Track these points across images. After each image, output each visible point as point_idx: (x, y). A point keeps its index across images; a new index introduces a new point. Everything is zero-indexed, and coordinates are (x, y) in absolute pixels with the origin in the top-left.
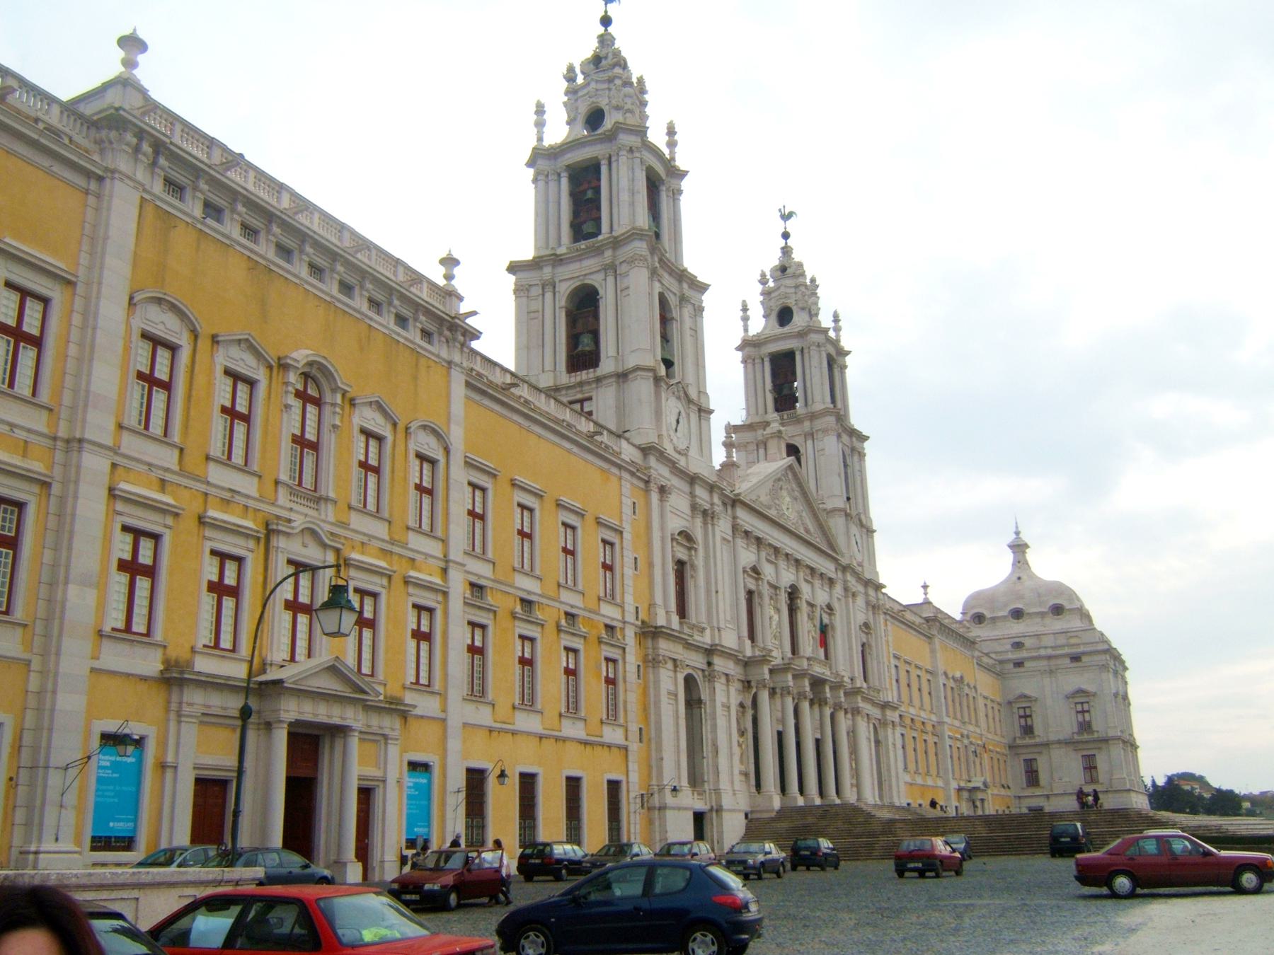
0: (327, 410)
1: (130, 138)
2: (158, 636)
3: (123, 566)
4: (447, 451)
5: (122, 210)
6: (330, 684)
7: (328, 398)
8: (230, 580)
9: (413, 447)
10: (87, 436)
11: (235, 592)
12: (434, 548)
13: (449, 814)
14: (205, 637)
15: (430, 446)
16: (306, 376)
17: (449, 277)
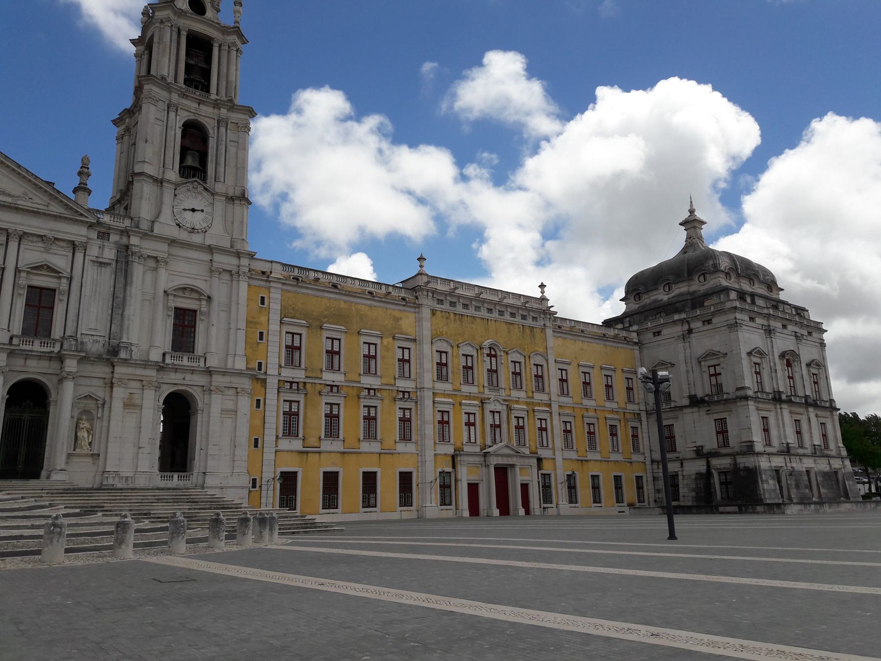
0: (499, 358)
1: (425, 293)
2: (452, 442)
3: (439, 422)
4: (547, 361)
5: (426, 313)
6: (507, 451)
7: (498, 354)
8: (472, 421)
9: (532, 362)
10: (425, 386)
11: (474, 424)
12: (544, 397)
13: (560, 491)
14: (465, 439)
15: (539, 360)
16: (490, 348)
17: (543, 292)
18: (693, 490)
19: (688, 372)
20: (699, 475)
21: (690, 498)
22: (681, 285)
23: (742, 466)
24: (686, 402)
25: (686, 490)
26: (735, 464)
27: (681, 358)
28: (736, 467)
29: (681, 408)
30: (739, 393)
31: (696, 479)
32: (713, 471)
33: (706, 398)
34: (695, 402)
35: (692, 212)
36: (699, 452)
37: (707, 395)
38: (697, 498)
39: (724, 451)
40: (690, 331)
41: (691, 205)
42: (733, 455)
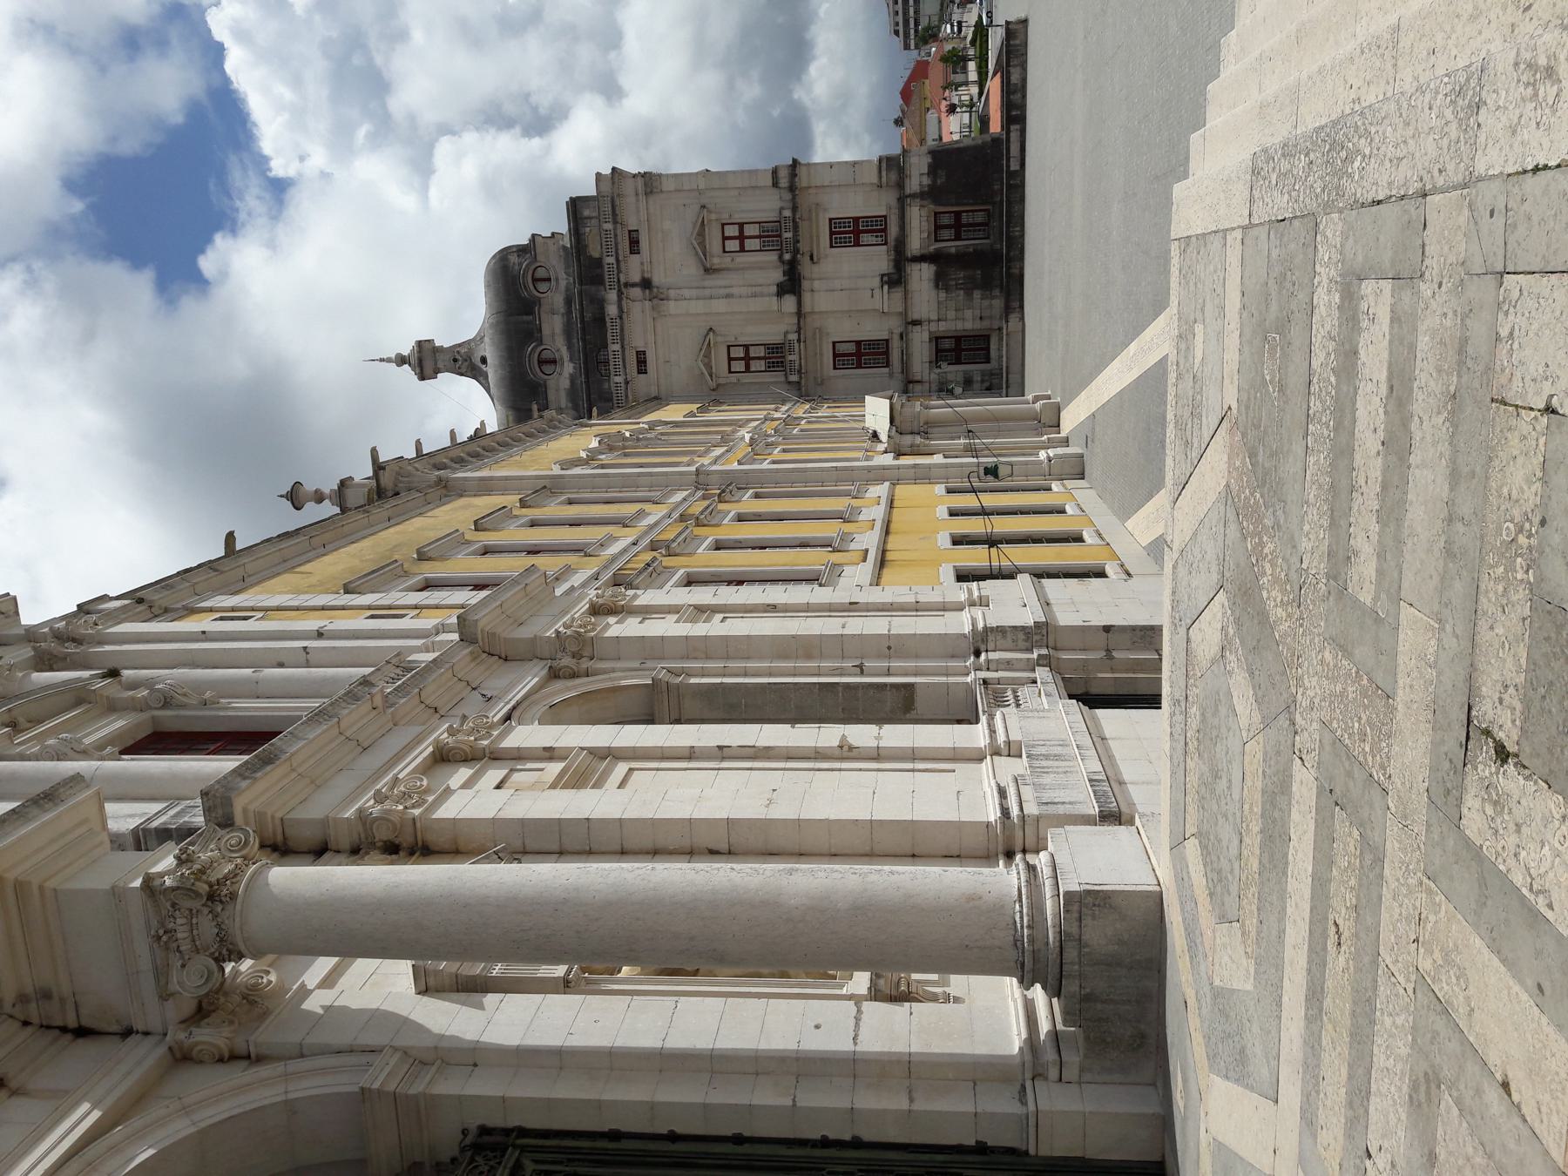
18: (969, 294)
19: (728, 296)
20: (940, 281)
21: (986, 303)
22: (546, 331)
23: (926, 181)
24: (789, 302)
25: (968, 313)
26: (922, 195)
27: (697, 307)
28: (931, 194)
29: (800, 314)
30: (784, 182)
31: (947, 289)
32: (932, 248)
33: (787, 257)
34: (791, 284)
35: (401, 360)
36: (895, 279)
37: (780, 257)
38: (986, 285)
39: (893, 230)
40: (646, 284)
41: (389, 360)
42: (902, 201)
